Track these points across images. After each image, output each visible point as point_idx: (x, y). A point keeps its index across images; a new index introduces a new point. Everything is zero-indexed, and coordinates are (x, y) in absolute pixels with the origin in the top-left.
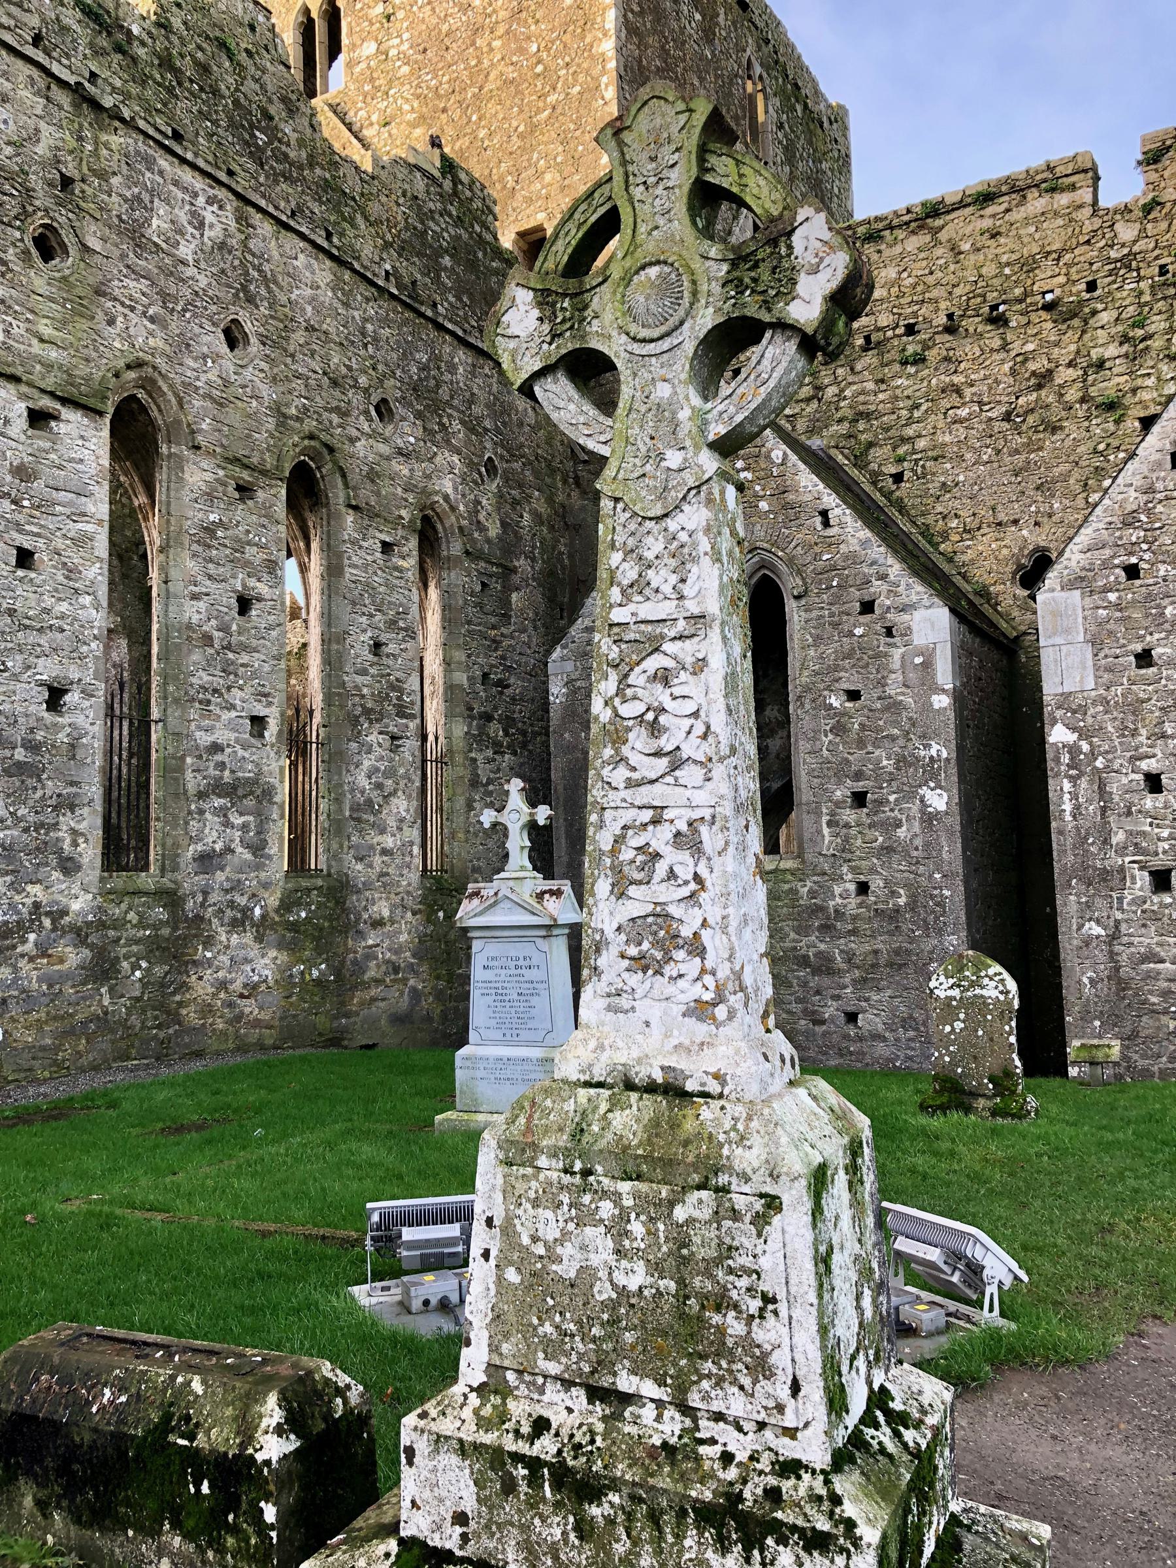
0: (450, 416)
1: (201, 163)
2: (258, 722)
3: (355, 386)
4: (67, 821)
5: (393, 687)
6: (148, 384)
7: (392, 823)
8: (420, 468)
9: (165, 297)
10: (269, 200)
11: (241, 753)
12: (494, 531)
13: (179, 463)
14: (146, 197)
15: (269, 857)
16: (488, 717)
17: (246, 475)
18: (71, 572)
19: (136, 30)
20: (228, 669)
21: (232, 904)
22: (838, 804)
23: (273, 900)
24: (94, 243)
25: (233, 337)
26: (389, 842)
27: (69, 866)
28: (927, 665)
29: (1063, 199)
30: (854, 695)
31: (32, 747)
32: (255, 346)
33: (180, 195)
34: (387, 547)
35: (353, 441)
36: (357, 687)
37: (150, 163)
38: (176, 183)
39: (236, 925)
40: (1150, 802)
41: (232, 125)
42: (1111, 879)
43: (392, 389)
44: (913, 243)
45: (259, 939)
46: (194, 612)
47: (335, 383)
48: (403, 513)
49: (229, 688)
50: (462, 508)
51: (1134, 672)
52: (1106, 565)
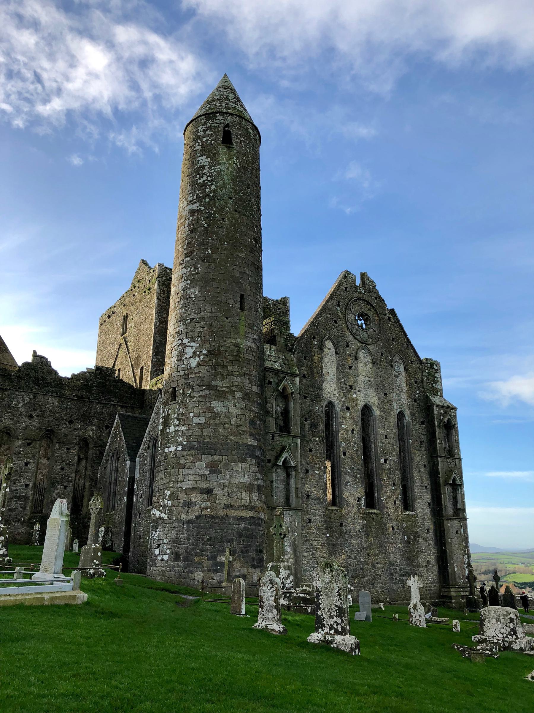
0: (93, 419)
1: (25, 391)
2: (27, 485)
3: (63, 419)
5: (66, 476)
6: (9, 430)
8: (81, 432)
9: (14, 415)
10: (41, 392)
11: (22, 490)
13: (14, 441)
14: (12, 399)
15: (27, 510)
17: (29, 441)
19: (12, 374)
21: (16, 518)
23: (27, 518)
25: (31, 417)
33: (20, 397)
34: (68, 449)
35: (60, 430)
36: (55, 477)
38: (19, 395)
39: (16, 522)
41: (33, 382)
43: (74, 417)
45: (22, 525)
47: (57, 420)
48: (74, 441)
49: (20, 479)
50: (95, 437)
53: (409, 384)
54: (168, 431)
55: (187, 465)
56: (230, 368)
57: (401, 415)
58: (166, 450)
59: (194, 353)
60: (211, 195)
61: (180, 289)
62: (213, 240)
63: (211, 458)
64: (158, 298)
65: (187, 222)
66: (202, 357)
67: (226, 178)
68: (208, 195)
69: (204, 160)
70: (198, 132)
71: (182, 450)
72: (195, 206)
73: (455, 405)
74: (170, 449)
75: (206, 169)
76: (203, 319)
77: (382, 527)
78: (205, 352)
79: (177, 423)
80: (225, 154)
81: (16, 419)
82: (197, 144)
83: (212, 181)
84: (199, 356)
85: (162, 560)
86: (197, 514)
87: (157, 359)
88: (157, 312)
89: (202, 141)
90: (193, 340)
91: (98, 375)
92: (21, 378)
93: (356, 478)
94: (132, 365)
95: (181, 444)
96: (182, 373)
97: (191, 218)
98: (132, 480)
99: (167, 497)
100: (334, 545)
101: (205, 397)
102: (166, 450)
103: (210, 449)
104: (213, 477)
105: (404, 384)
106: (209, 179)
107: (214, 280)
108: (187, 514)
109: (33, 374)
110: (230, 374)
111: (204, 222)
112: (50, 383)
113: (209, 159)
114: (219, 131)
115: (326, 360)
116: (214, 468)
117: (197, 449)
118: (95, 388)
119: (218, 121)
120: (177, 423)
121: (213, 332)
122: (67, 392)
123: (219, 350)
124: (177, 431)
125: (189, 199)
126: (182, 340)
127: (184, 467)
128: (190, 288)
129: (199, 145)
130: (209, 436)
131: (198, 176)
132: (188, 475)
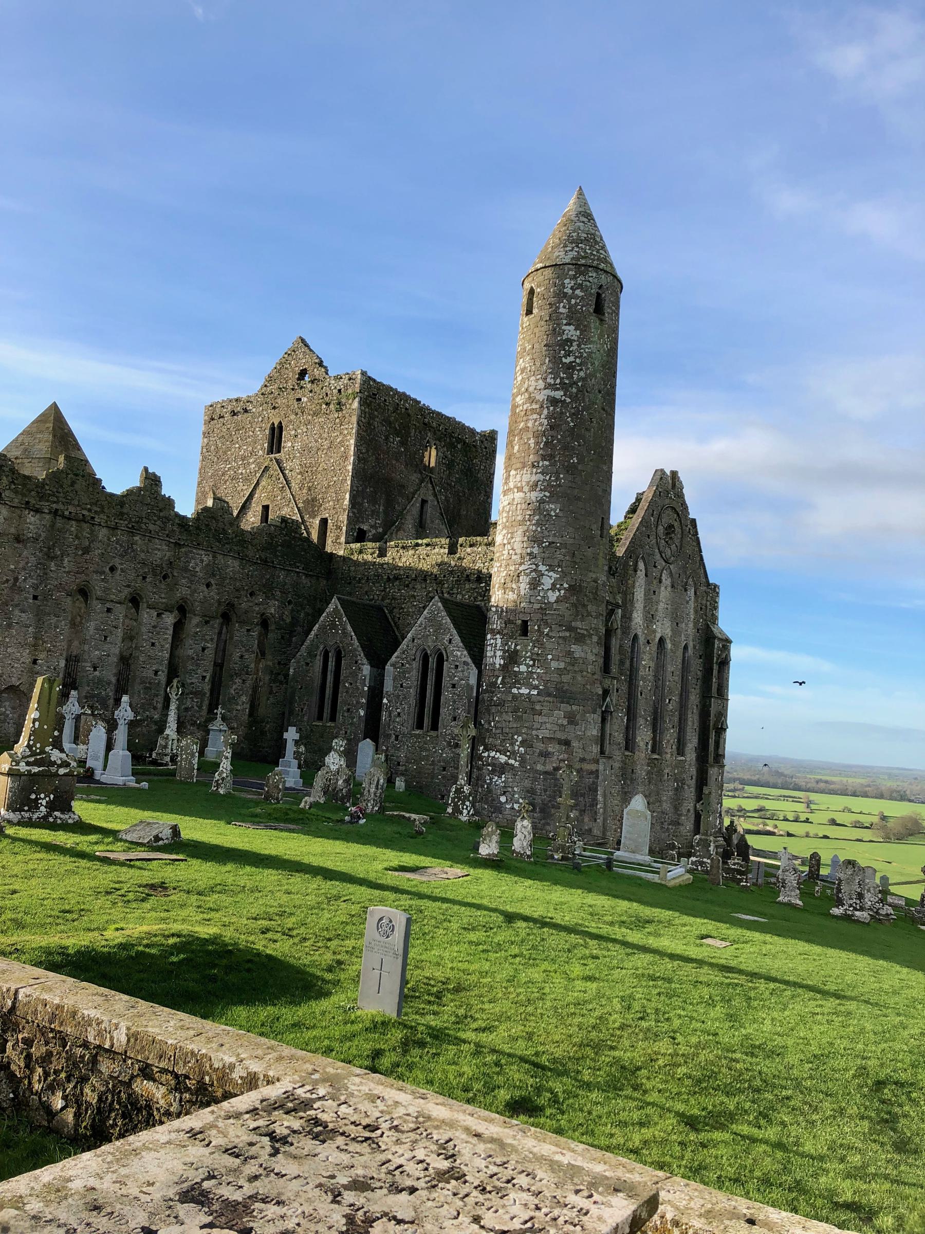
2: (204, 677)
4: (156, 699)
6: (185, 602)
7: (240, 703)
9: (191, 582)
12: (288, 620)
13: (191, 618)
16: (279, 674)
18: (162, 646)
20: (198, 665)
24: (176, 574)
26: (239, 708)
27: (155, 708)
29: (442, 551)
31: (150, 683)
32: (214, 587)
37: (191, 552)
39: (192, 725)
42: (389, 736)
43: (256, 587)
44: (411, 552)
46: (190, 652)
47: (237, 590)
53: (696, 612)
54: (516, 669)
55: (544, 712)
56: (589, 608)
57: (686, 647)
58: (515, 691)
59: (554, 585)
60: (580, 384)
61: (534, 499)
62: (579, 445)
63: (569, 708)
64: (358, 423)
65: (545, 412)
66: (562, 592)
67: (597, 363)
68: (575, 383)
69: (571, 332)
70: (564, 288)
71: (538, 694)
72: (558, 394)
73: (731, 637)
74: (521, 691)
75: (574, 348)
76: (564, 545)
77: (660, 773)
78: (566, 585)
79: (531, 663)
80: (597, 329)
81: (193, 587)
82: (562, 305)
83: (580, 365)
84: (559, 591)
85: (513, 808)
86: (554, 765)
87: (353, 513)
88: (356, 445)
89: (569, 302)
90: (551, 568)
91: (283, 529)
92: (200, 530)
93: (647, 720)
94: (299, 510)
95: (536, 687)
96: (537, 606)
97: (552, 408)
98: (376, 692)
99: (518, 743)
100: (626, 793)
101: (564, 638)
102: (515, 691)
103: (570, 698)
104: (570, 728)
105: (692, 611)
106: (578, 361)
107: (578, 499)
108: (544, 764)
109: (213, 525)
110: (589, 614)
111: (569, 419)
112: (232, 539)
113: (578, 333)
114: (591, 294)
115: (637, 584)
116: (572, 719)
117: (555, 696)
118: (280, 548)
119: (590, 279)
120: (531, 663)
121: (575, 563)
122: (250, 552)
123: (580, 585)
124: (532, 673)
125: (548, 380)
126: (537, 565)
127: (540, 714)
128: (549, 503)
129: (564, 307)
130: (569, 683)
131: (563, 352)
132: (545, 723)
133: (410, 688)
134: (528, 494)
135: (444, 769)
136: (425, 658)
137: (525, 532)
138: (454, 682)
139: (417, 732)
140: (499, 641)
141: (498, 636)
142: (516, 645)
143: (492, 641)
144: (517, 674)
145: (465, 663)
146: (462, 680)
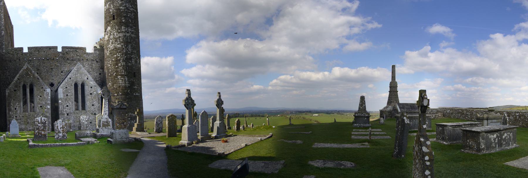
22: (39, 107)
28: (48, 94)
30: (41, 96)
40: (67, 108)
51: (66, 96)
52: (64, 86)
54: (134, 87)
96: (137, 68)
102: (134, 94)
126: (136, 56)
133: (72, 95)
134: (131, 35)
135: (91, 123)
136: (76, 85)
137: (131, 46)
138: (91, 93)
139: (77, 111)
140: (126, 78)
141: (126, 77)
142: (133, 80)
143: (122, 78)
144: (135, 89)
145: (95, 86)
146: (94, 92)
